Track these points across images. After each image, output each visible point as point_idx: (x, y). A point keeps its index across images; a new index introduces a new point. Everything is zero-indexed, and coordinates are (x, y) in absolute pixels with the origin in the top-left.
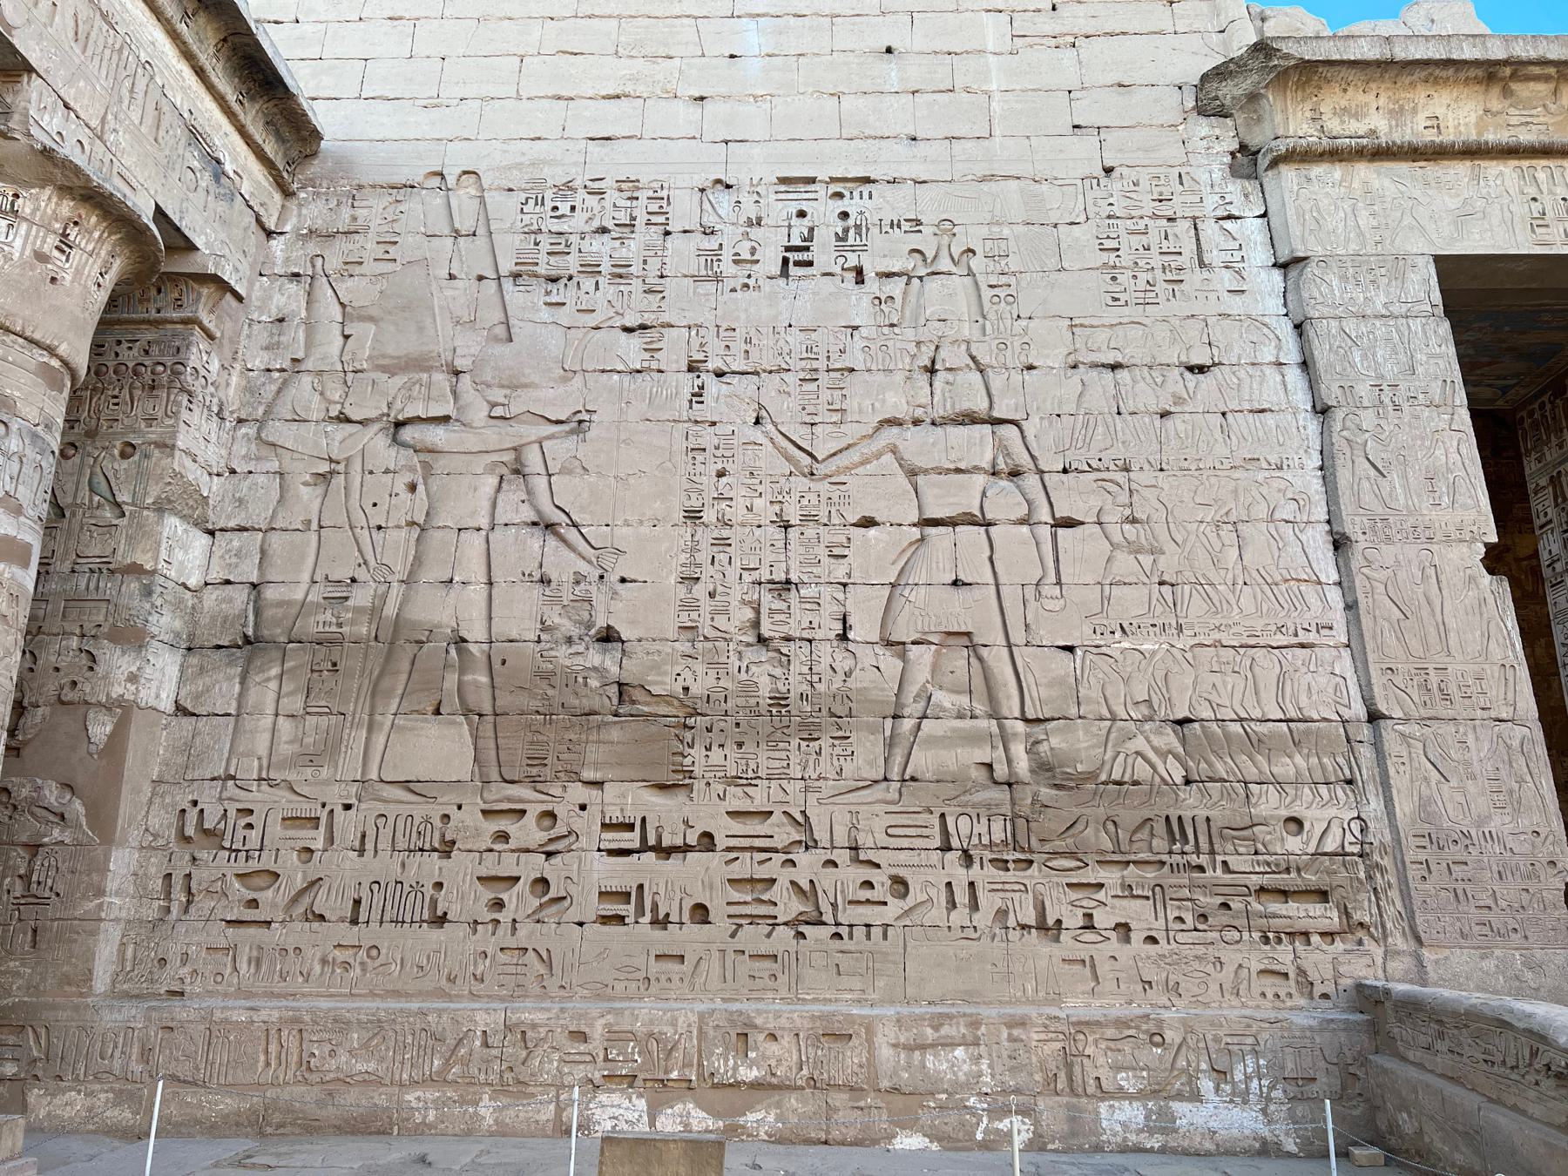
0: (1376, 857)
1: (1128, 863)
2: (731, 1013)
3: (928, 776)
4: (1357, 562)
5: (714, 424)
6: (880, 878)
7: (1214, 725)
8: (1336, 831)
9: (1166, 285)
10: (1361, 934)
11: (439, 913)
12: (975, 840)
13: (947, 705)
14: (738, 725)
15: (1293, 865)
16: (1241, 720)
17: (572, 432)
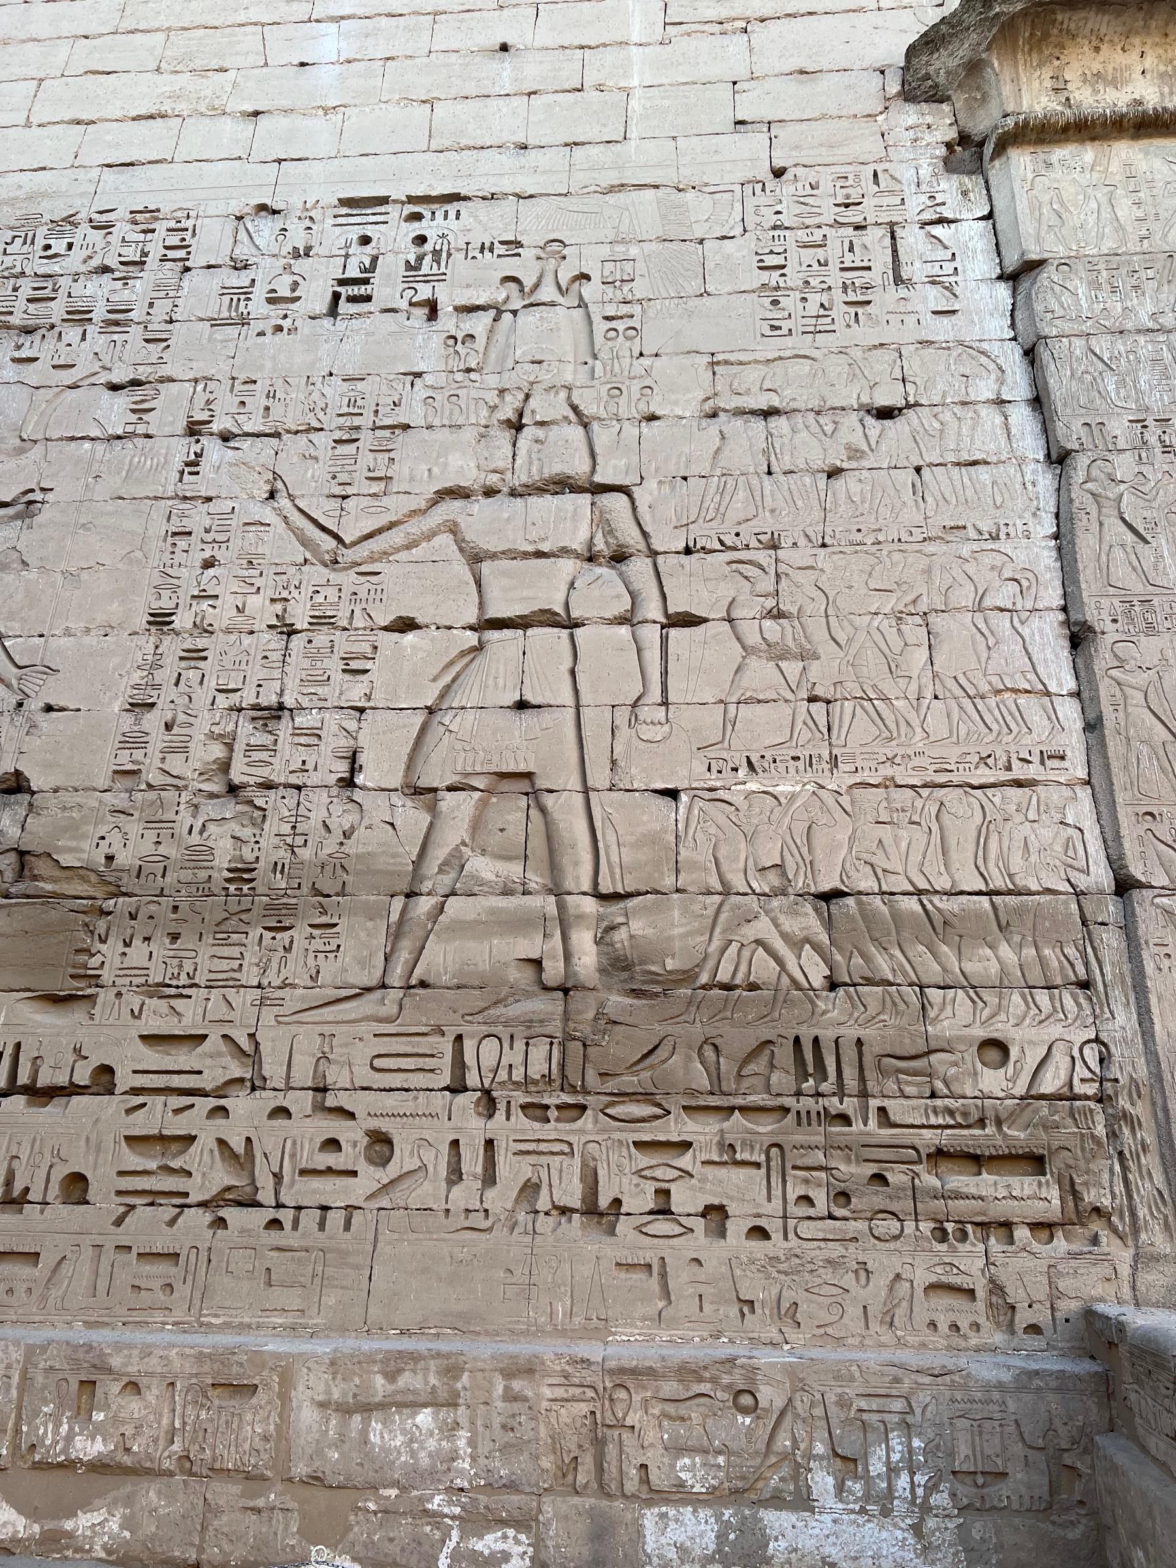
0: (1123, 1102)
1: (731, 1109)
2: (76, 1347)
3: (445, 979)
4: (1102, 659)
6: (351, 1135)
7: (877, 901)
8: (1060, 1061)
9: (846, 308)
10: (1097, 1226)
12: (503, 1075)
13: (489, 876)
14: (176, 908)
15: (990, 1114)
16: (920, 892)
17: (17, 516)
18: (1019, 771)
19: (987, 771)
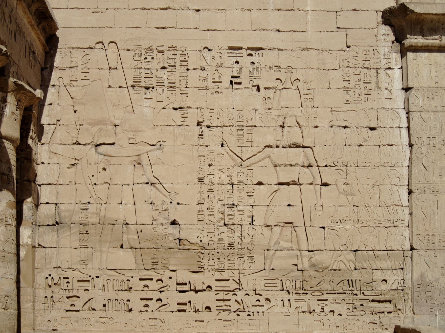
5: (207, 146)
6: (262, 299)
7: (365, 252)
8: (396, 283)
10: (399, 312)
11: (130, 308)
12: (291, 287)
15: (383, 293)
16: (373, 250)
18: (395, 224)
19: (389, 224)
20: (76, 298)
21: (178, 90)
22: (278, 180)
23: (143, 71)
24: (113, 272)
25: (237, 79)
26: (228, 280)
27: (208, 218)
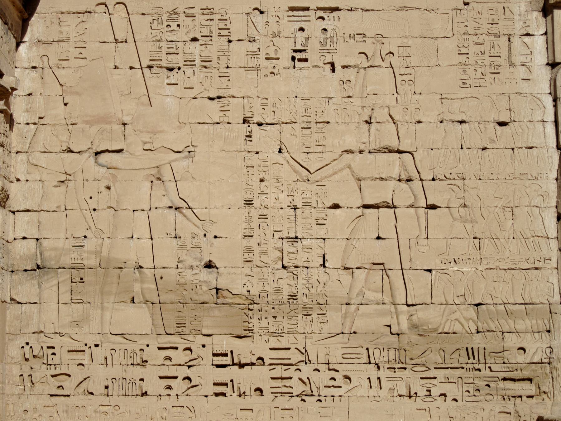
5: (257, 153)
7: (492, 307)
10: (544, 396)
11: (144, 392)
12: (382, 359)
16: (504, 304)
17: (186, 157)
18: (537, 265)
20: (64, 376)
21: (215, 71)
22: (363, 201)
23: (164, 44)
24: (119, 339)
25: (301, 54)
26: (289, 349)
27: (259, 258)
